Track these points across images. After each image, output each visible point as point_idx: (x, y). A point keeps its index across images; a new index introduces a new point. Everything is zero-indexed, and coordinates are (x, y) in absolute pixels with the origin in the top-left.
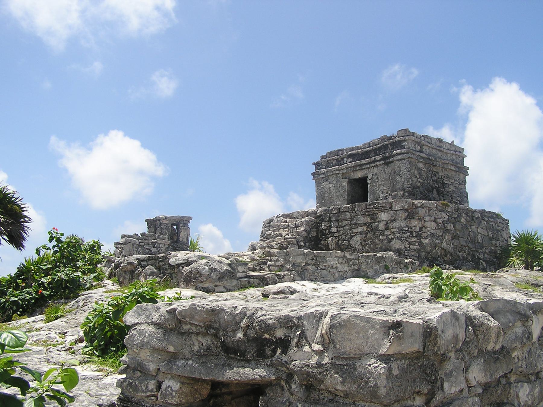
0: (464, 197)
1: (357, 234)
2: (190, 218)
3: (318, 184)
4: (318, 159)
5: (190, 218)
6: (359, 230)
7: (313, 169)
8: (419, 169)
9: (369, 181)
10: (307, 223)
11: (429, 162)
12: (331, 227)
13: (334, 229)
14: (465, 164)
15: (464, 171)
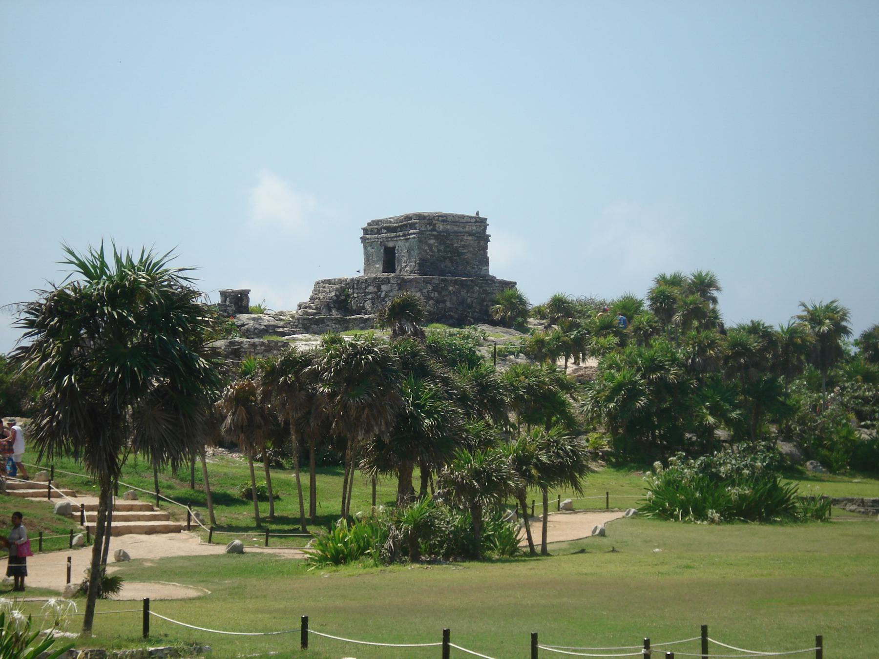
0: (485, 261)
1: (369, 299)
2: (250, 291)
3: (365, 248)
4: (365, 225)
5: (250, 291)
6: (370, 296)
7: (361, 234)
8: (430, 246)
9: (396, 252)
10: (337, 290)
11: (442, 238)
12: (354, 293)
13: (355, 295)
14: (488, 233)
15: (486, 239)
